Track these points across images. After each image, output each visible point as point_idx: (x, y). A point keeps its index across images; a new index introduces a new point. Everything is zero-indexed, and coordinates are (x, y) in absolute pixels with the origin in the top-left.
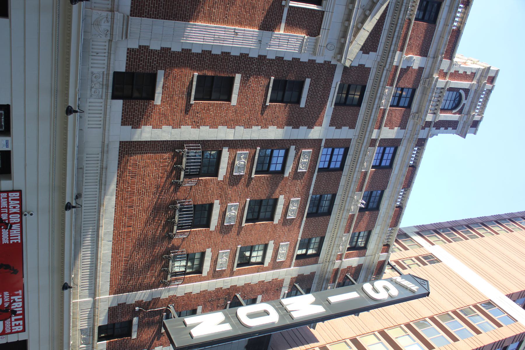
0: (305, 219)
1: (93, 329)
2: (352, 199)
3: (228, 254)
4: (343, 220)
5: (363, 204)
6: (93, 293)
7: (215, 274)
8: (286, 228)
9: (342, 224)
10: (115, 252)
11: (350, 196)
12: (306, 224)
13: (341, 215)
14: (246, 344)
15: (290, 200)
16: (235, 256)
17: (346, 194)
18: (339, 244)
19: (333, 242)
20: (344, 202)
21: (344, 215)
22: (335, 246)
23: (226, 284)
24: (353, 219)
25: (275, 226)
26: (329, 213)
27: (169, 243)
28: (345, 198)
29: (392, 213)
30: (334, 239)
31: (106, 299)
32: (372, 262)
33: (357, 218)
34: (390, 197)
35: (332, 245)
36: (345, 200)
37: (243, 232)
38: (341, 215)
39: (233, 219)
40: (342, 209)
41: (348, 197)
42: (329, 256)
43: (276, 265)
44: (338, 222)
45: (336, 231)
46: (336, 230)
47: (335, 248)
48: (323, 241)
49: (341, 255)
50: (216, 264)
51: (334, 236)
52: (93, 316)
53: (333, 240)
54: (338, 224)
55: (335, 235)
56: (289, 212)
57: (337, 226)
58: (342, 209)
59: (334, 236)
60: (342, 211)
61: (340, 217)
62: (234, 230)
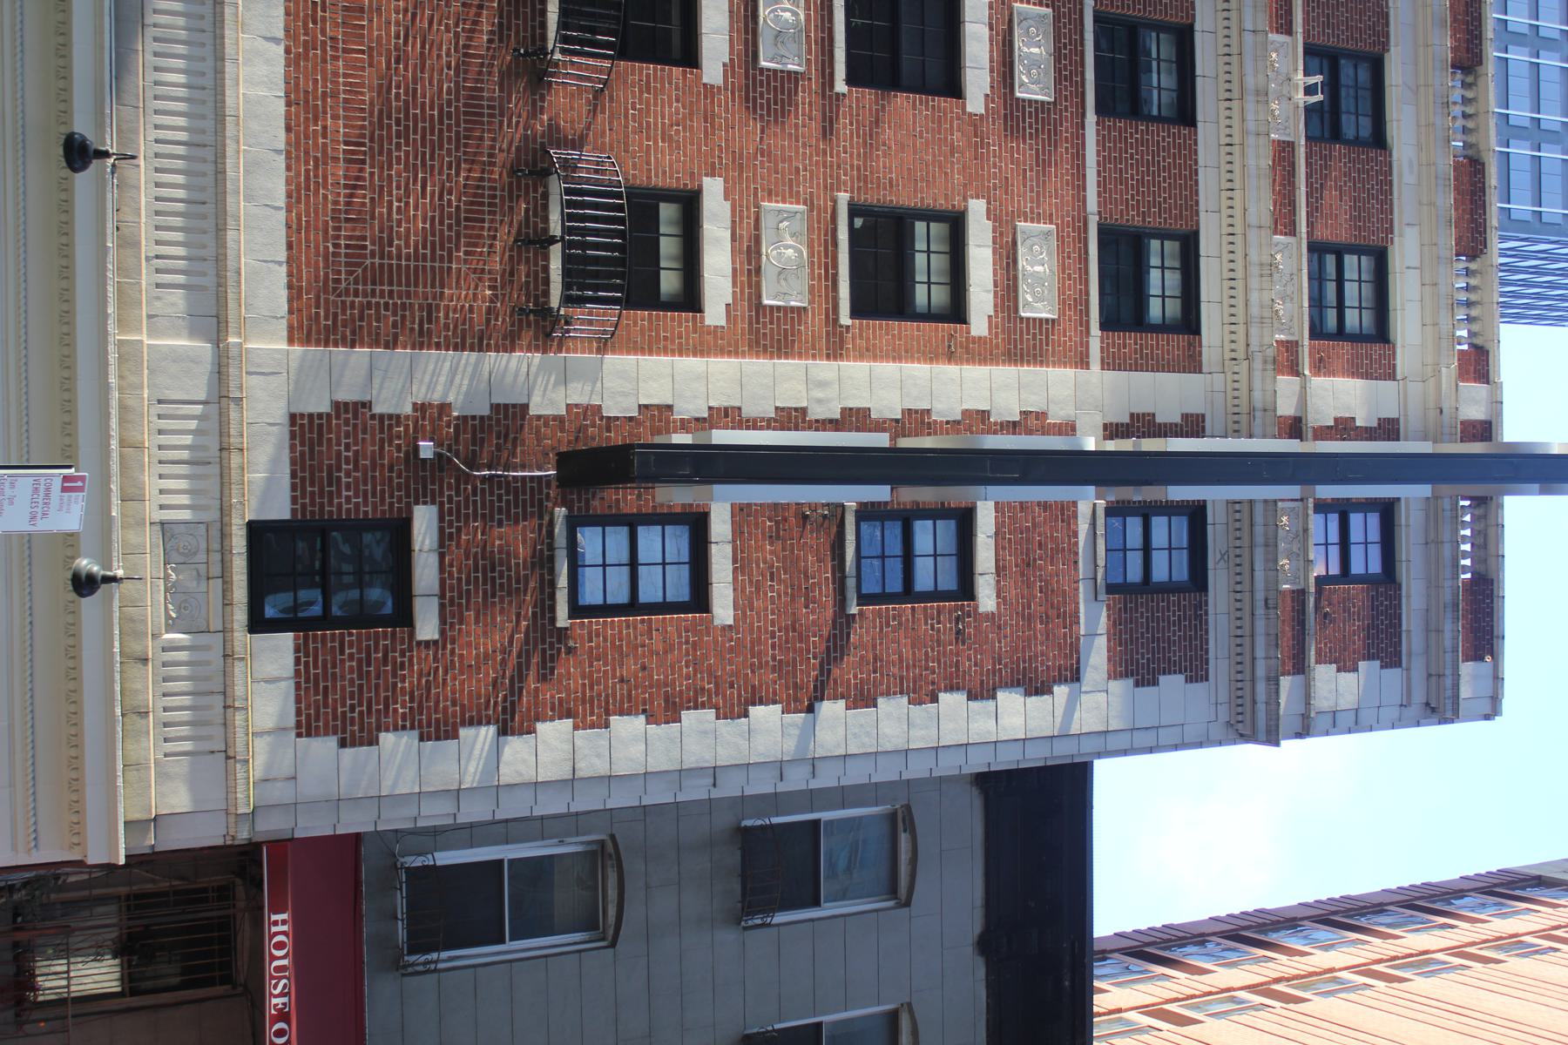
0: (1091, 118)
1: (224, 535)
2: (1260, 38)
3: (800, 225)
4: (1251, 140)
5: (1309, 90)
6: (213, 316)
7: (766, 331)
8: (1025, 151)
9: (1251, 162)
10: (302, 103)
11: (1248, 25)
12: (1101, 143)
13: (1236, 122)
14: (978, 928)
15: (1011, 9)
16: (835, 244)
17: (1234, 24)
18: (1266, 259)
19: (1239, 257)
20: (1235, 60)
21: (1250, 116)
22: (1254, 270)
23: (819, 394)
24: (1293, 165)
25: (975, 121)
26: (1185, 114)
27: (535, 112)
28: (1234, 41)
29: (1447, 200)
30: (1238, 239)
31: (279, 372)
32: (1433, 414)
33: (1308, 164)
34: (1416, 93)
35: (1239, 274)
36: (1234, 50)
37: (844, 125)
38: (1236, 122)
39: (794, 47)
40: (1236, 94)
41: (1242, 30)
42: (1241, 329)
43: (1021, 342)
44: (1236, 158)
45: (1237, 203)
46: (1237, 194)
47: (1254, 283)
48: (1197, 256)
49: (1291, 347)
50: (758, 270)
51: (1238, 229)
52: (215, 456)
53: (1239, 248)
54: (1237, 167)
55: (1238, 221)
56: (1018, 68)
57: (1237, 176)
58: (1236, 94)
59: (1238, 229)
60: (1235, 105)
61: (1236, 131)
62: (805, 97)
